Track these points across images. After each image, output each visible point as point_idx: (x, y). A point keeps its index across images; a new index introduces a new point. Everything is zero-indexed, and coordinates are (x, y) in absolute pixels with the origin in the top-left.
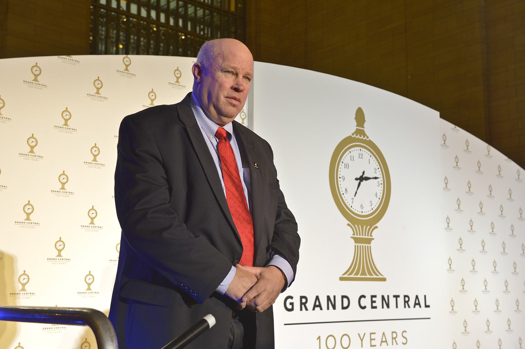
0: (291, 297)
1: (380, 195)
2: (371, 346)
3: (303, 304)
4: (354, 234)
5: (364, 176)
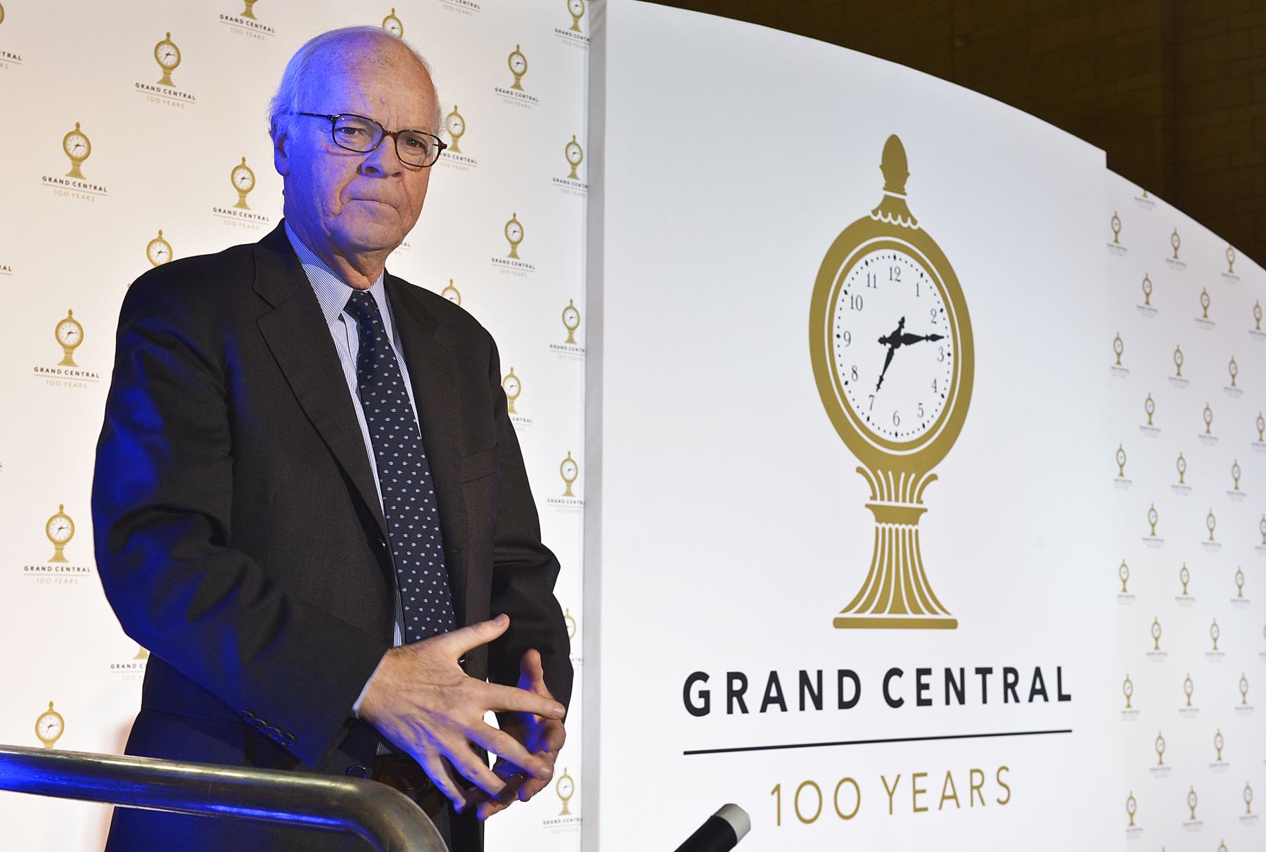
0: (703, 677)
1: (945, 386)
2: (916, 810)
3: (735, 696)
4: (873, 498)
5: (903, 332)
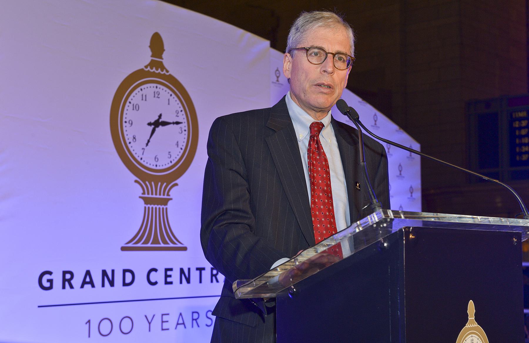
0: (50, 273)
2: (163, 329)
4: (144, 193)
5: (160, 120)
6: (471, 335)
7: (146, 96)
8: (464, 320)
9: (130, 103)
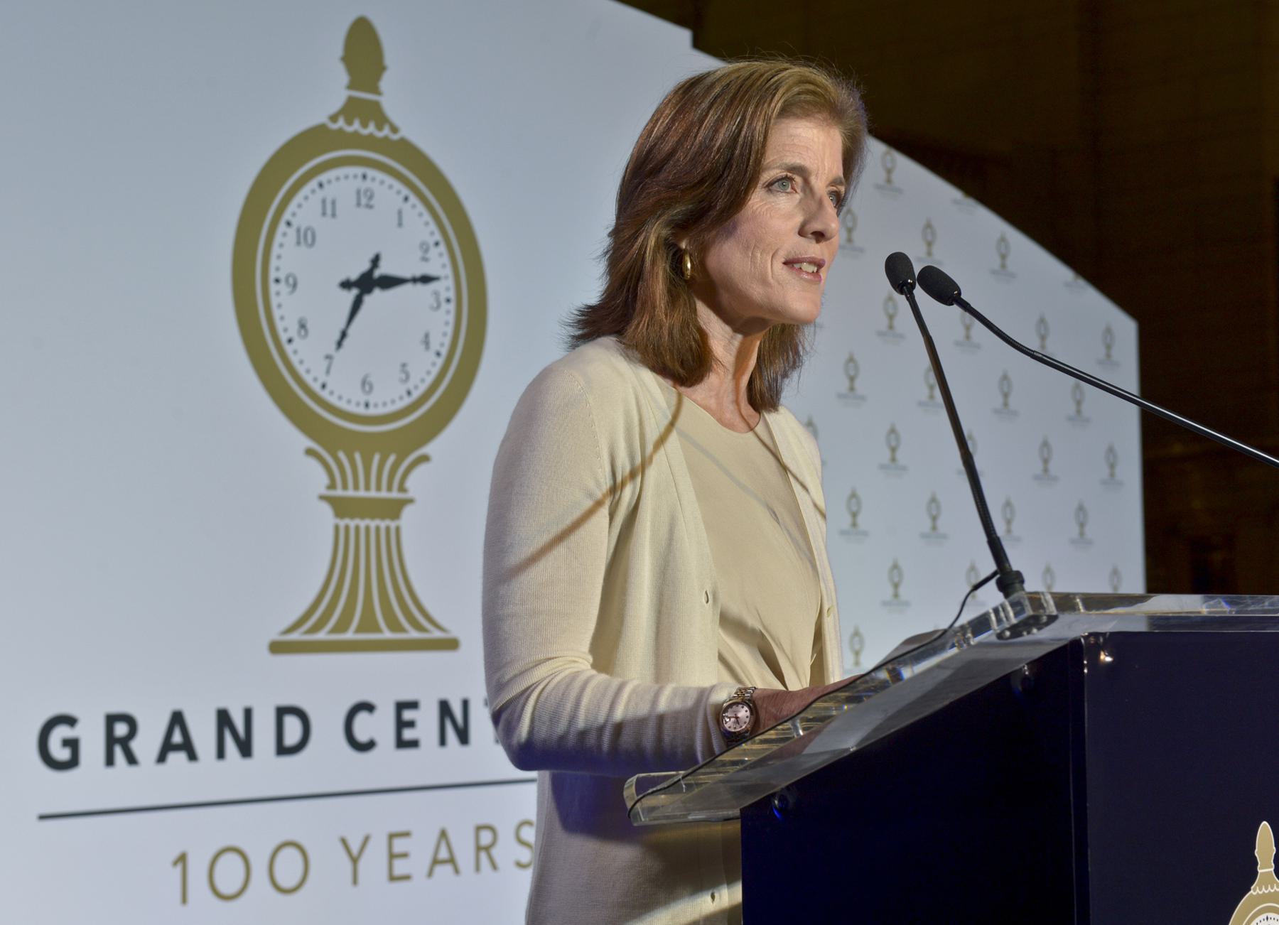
0: (70, 721)
1: (441, 341)
2: (393, 878)
4: (332, 486)
5: (377, 273)
6: (1264, 916)
7: (334, 203)
8: (1248, 875)
9: (289, 224)
